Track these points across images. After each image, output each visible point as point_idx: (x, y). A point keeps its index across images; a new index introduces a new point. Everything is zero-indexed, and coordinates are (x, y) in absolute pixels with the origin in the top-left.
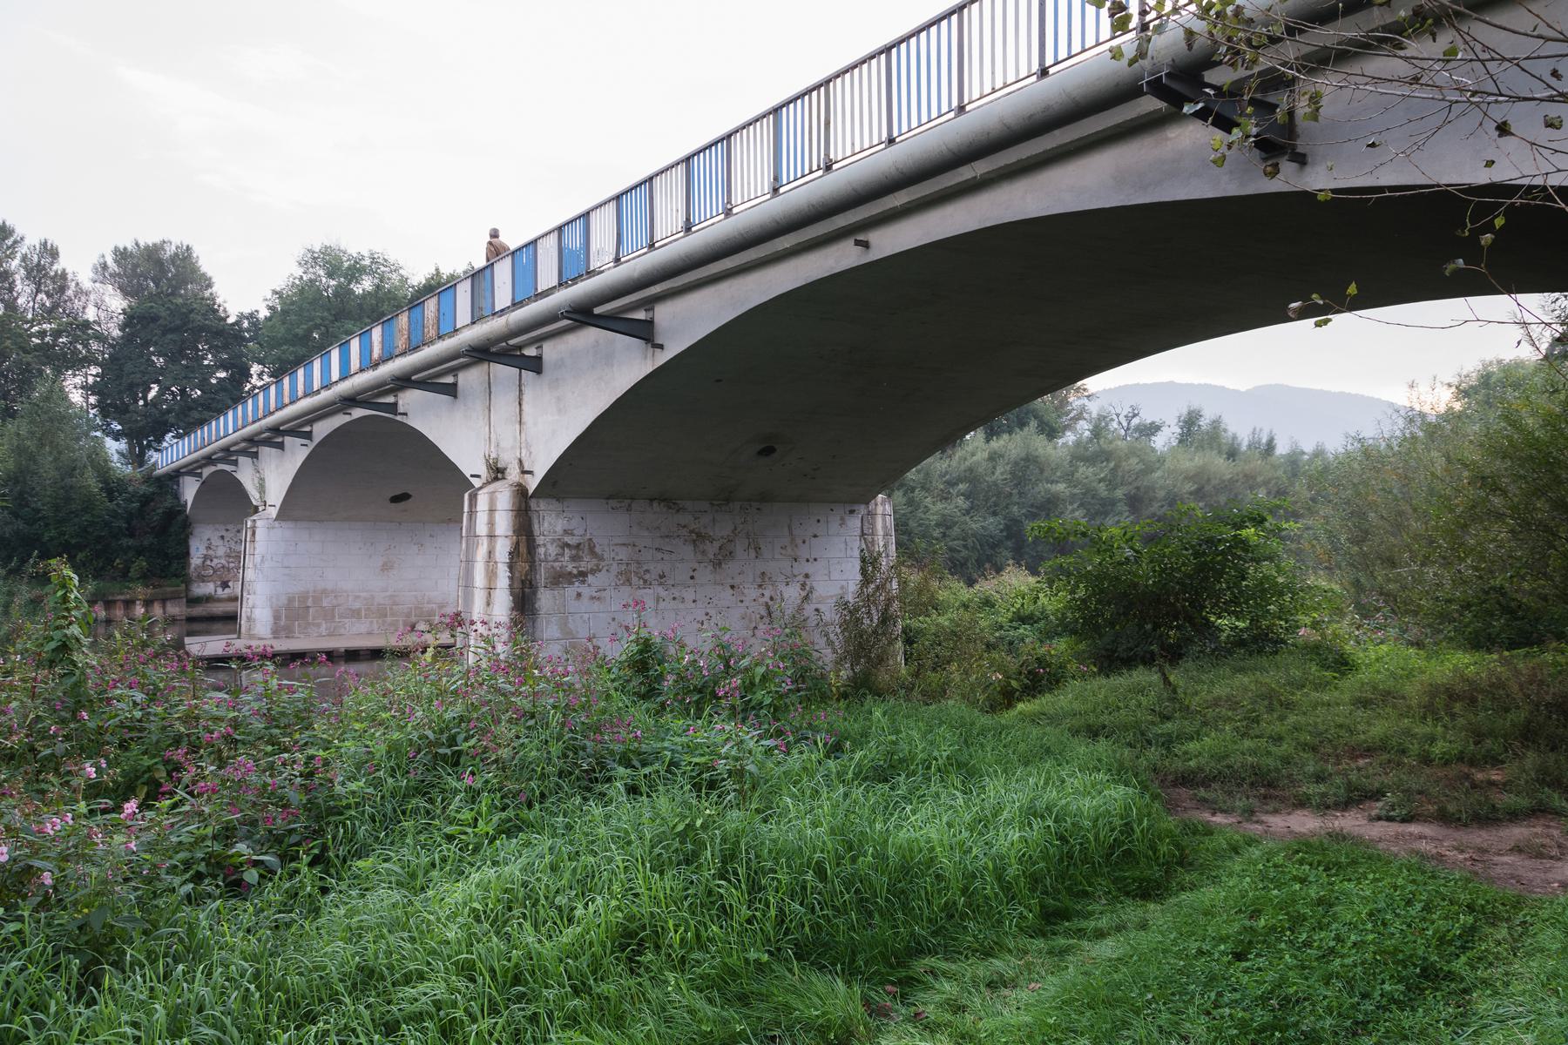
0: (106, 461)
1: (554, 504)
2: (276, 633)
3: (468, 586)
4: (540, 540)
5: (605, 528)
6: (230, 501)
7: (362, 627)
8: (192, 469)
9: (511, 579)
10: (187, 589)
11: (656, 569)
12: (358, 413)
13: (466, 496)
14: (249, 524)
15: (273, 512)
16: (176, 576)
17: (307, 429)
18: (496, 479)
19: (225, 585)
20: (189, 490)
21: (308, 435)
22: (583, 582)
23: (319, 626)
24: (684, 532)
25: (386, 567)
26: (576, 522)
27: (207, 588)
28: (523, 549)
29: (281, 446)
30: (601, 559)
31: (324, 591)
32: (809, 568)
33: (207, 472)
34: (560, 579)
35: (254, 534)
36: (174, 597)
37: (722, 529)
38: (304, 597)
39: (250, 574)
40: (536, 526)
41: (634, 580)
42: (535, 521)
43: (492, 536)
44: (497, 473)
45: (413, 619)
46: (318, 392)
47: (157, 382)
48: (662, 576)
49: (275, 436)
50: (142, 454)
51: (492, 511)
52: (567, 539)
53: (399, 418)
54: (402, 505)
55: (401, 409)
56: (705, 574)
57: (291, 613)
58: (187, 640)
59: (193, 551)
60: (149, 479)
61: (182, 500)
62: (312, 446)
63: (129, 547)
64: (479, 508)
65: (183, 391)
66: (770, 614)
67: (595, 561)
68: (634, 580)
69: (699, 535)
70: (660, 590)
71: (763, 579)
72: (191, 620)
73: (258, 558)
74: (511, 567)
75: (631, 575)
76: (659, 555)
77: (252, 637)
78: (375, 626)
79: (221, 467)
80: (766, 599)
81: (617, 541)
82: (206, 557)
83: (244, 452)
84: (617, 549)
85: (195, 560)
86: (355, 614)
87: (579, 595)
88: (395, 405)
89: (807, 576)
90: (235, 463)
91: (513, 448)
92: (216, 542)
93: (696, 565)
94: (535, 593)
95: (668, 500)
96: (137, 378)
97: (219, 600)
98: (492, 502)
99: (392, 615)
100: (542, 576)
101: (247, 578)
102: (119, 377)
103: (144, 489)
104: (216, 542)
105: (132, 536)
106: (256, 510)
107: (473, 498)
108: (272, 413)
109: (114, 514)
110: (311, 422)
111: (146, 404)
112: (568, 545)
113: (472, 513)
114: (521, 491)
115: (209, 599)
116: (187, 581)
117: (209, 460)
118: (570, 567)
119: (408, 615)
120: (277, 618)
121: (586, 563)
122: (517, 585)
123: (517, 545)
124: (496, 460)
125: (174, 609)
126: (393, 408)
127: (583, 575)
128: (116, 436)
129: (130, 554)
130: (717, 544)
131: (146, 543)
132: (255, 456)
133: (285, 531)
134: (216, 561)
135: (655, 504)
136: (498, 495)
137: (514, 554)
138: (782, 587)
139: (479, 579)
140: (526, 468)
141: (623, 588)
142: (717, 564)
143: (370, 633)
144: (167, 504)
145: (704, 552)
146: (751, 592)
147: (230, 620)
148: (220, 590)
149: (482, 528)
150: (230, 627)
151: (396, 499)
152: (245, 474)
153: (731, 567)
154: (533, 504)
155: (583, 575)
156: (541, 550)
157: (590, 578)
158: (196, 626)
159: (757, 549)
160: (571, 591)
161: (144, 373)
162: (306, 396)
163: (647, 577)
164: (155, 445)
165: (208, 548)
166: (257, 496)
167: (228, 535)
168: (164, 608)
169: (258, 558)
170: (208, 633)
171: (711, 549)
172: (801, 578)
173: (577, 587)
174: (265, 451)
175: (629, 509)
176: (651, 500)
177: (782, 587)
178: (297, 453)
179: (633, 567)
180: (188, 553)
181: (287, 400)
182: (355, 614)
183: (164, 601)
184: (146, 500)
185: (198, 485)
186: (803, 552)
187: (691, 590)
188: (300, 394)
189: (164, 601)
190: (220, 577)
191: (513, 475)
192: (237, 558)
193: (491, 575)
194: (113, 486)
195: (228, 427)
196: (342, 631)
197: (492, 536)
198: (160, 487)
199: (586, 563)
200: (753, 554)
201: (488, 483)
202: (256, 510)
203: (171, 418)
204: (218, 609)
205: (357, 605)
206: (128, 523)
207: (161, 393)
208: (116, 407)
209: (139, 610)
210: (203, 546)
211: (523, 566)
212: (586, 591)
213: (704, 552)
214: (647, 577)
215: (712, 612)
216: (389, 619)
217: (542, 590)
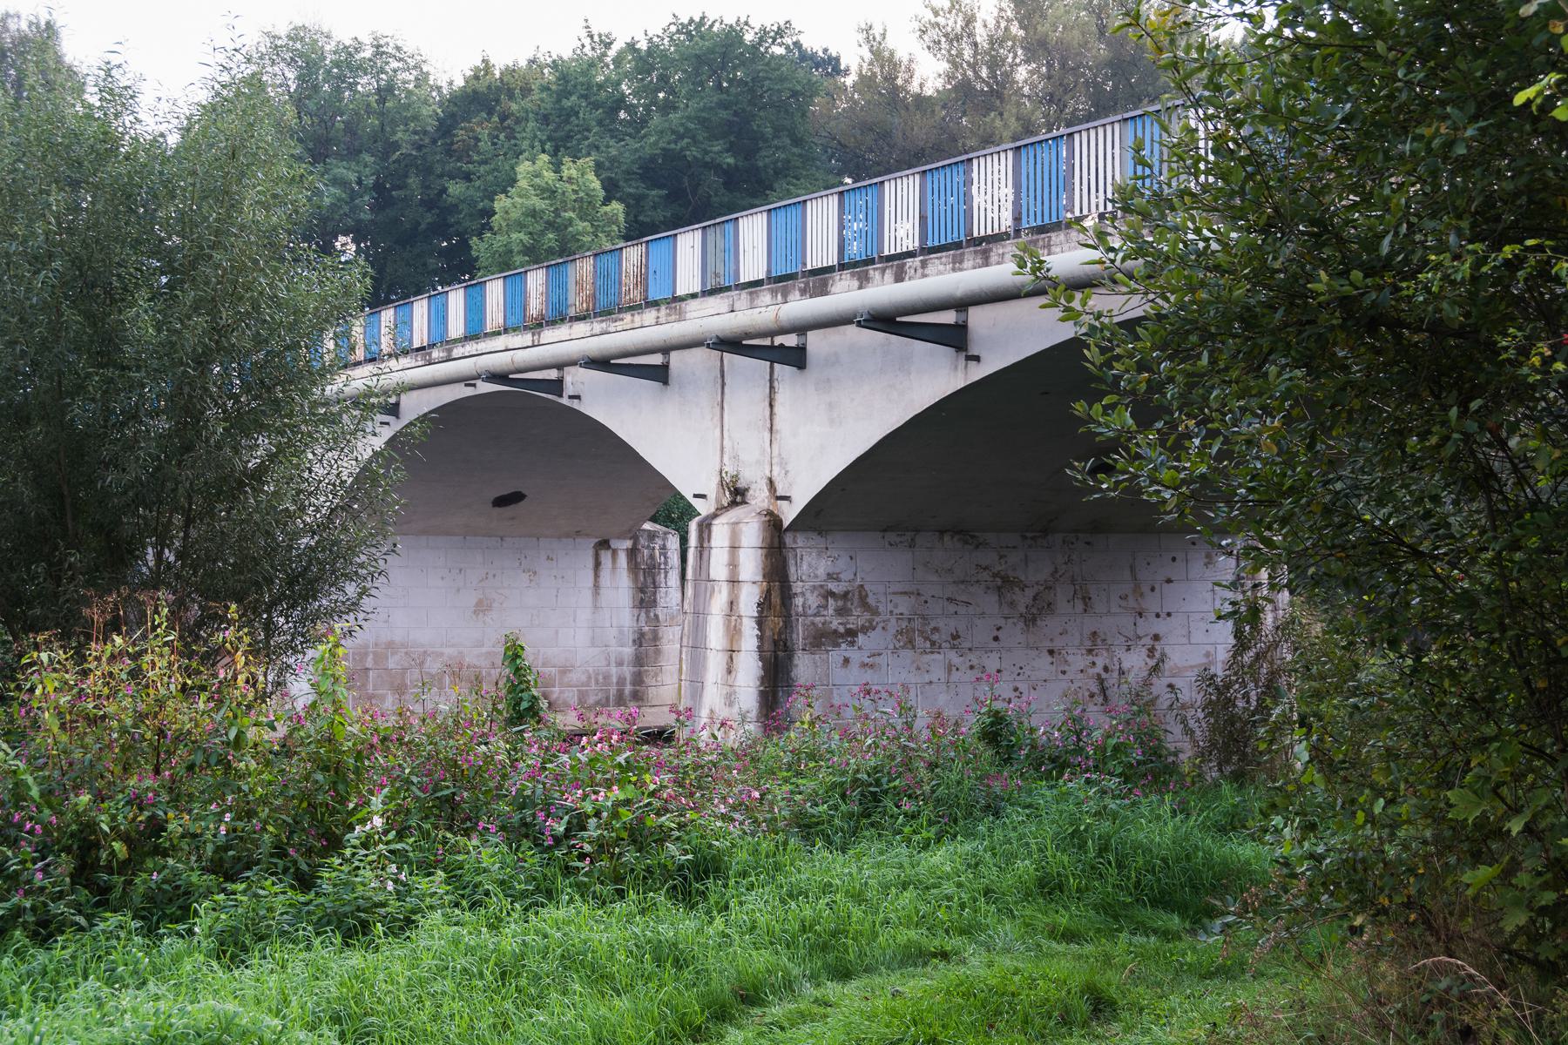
4: (797, 587)
5: (876, 569)
9: (761, 638)
11: (947, 626)
22: (852, 643)
24: (985, 575)
26: (843, 563)
28: (776, 599)
30: (875, 612)
32: (1160, 627)
34: (822, 639)
37: (1037, 572)
40: (792, 569)
41: (919, 641)
42: (791, 562)
43: (734, 582)
44: (737, 495)
48: (955, 637)
51: (734, 548)
52: (832, 586)
56: (1014, 633)
66: (1103, 690)
67: (867, 616)
68: (919, 641)
69: (1005, 579)
71: (1095, 642)
74: (760, 622)
76: (952, 608)
80: (1099, 669)
84: (898, 599)
87: (847, 661)
89: (1156, 637)
93: (1001, 622)
95: (964, 533)
100: (799, 635)
112: (832, 594)
114: (773, 523)
118: (835, 624)
121: (857, 619)
122: (768, 646)
124: (736, 478)
127: (851, 634)
130: (1030, 593)
135: (947, 538)
136: (743, 527)
137: (764, 605)
138: (1120, 653)
141: (903, 653)
142: (1030, 620)
145: (1012, 604)
146: (1078, 660)
153: (1050, 624)
154: (788, 539)
155: (851, 634)
156: (799, 601)
157: (861, 638)
159: (1086, 600)
160: (836, 656)
163: (935, 637)
171: (1023, 599)
172: (1148, 641)
173: (844, 650)
175: (912, 545)
176: (942, 532)
177: (1120, 653)
179: (917, 624)
186: (1151, 603)
187: (995, 656)
191: (759, 498)
193: (733, 632)
197: (734, 582)
199: (857, 619)
200: (1080, 606)
211: (775, 622)
212: (855, 656)
213: (1012, 604)
214: (935, 637)
215: (1023, 687)
217: (799, 653)
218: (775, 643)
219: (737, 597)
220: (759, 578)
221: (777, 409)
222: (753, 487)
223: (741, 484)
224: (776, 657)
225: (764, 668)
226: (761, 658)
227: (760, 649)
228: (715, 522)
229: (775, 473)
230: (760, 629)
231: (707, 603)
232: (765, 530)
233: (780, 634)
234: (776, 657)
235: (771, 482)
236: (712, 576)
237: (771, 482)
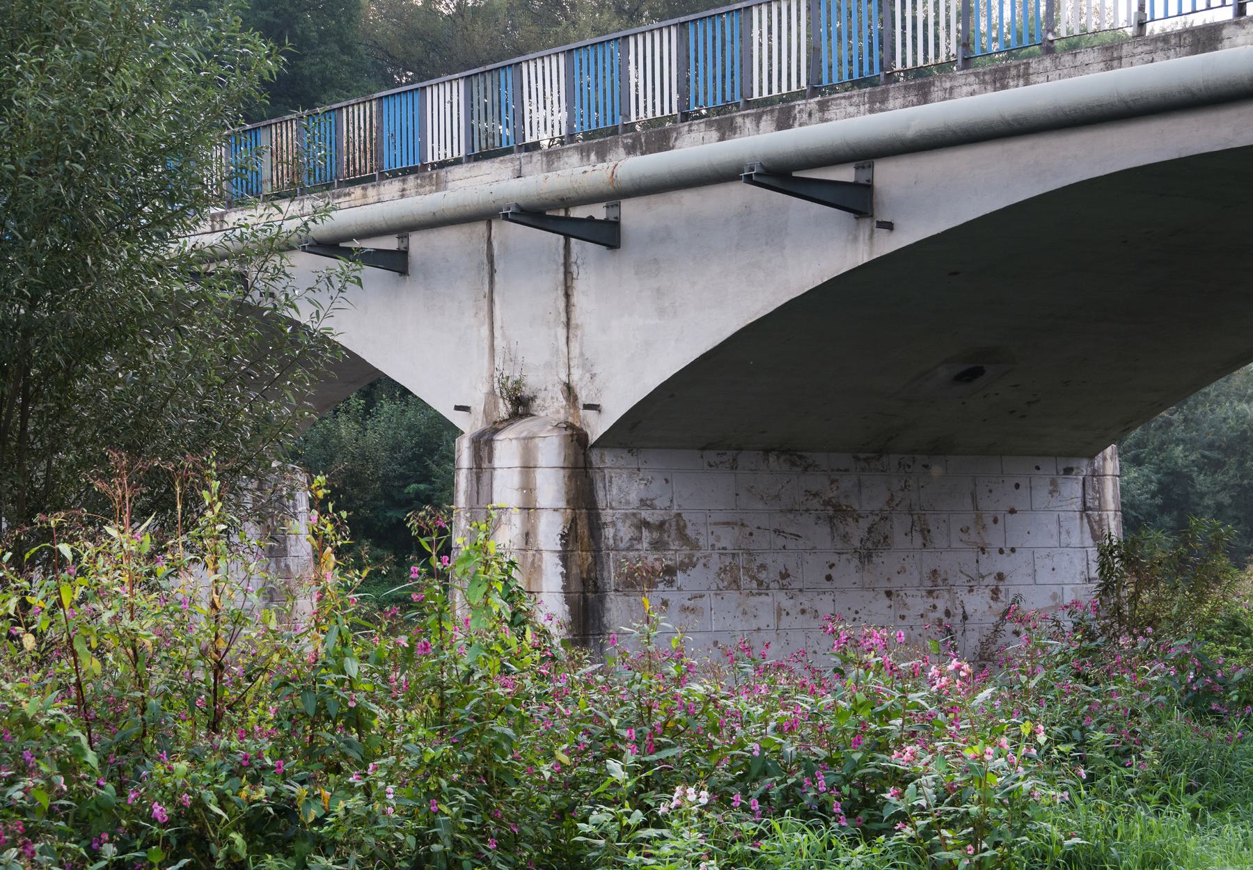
1: (625, 459)
4: (607, 516)
9: (566, 577)
22: (670, 583)
24: (815, 503)
28: (583, 529)
30: (695, 546)
37: (871, 501)
40: (600, 494)
41: (744, 580)
42: (599, 485)
48: (785, 575)
52: (646, 514)
56: (848, 571)
67: (686, 550)
68: (744, 580)
69: (838, 509)
70: (782, 598)
74: (565, 558)
75: (741, 575)
76: (780, 541)
81: (717, 517)
87: (665, 603)
93: (834, 558)
94: (601, 600)
95: (791, 452)
112: (646, 524)
122: (575, 586)
123: (573, 524)
127: (670, 571)
130: (864, 524)
136: (540, 443)
142: (865, 557)
145: (845, 537)
153: (887, 561)
154: (595, 456)
156: (609, 532)
159: (925, 532)
171: (857, 532)
175: (734, 466)
176: (767, 451)
179: (742, 560)
187: (827, 598)
211: (582, 557)
212: (674, 597)
213: (845, 537)
217: (612, 595)
220: (562, 504)
221: (574, 300)
224: (585, 599)
225: (571, 612)
226: (567, 601)
230: (565, 565)
232: (567, 446)
233: (589, 571)
234: (585, 599)
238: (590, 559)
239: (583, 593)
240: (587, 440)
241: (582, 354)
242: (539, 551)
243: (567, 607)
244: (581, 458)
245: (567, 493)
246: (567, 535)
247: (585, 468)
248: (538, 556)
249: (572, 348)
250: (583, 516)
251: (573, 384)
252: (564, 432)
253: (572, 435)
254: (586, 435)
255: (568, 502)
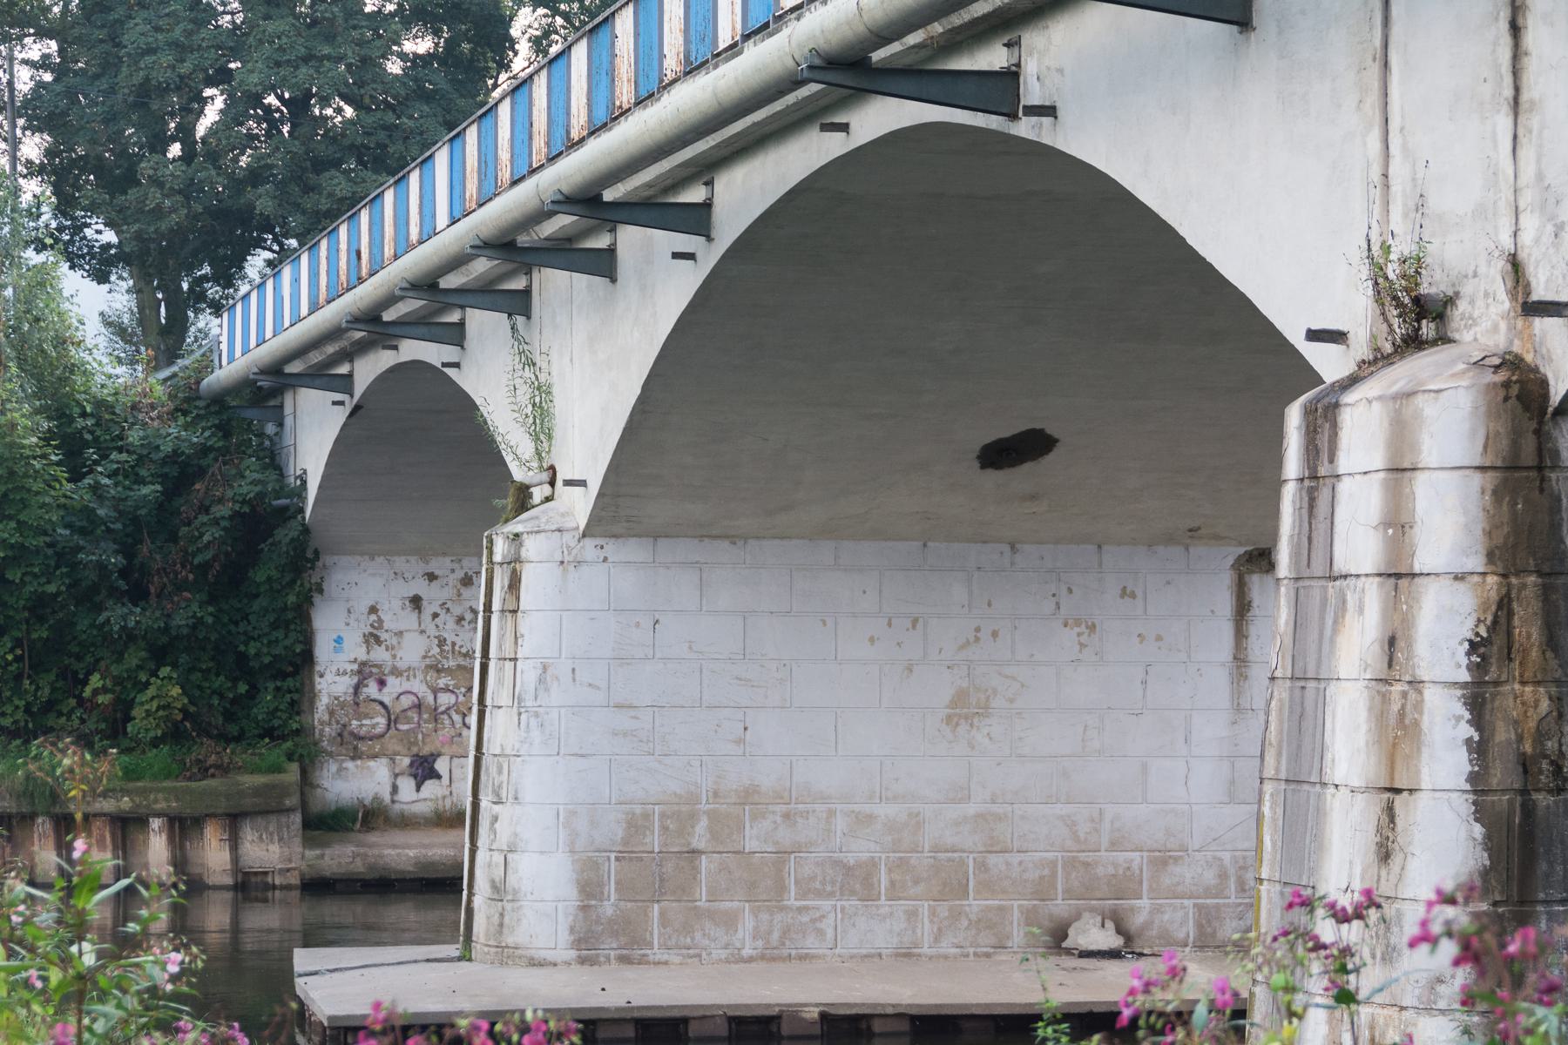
0: (61, 342)
2: (587, 948)
3: (1303, 779)
6: (438, 463)
7: (878, 929)
8: (319, 362)
9: (1479, 750)
10: (307, 781)
12: (879, 118)
13: (1294, 416)
14: (501, 549)
15: (578, 506)
16: (272, 734)
17: (695, 195)
18: (1413, 343)
19: (424, 769)
20: (313, 433)
21: (698, 220)
23: (730, 921)
25: (965, 710)
27: (356, 781)
29: (604, 265)
31: (749, 796)
33: (368, 370)
35: (514, 584)
36: (265, 808)
38: (681, 815)
39: (501, 730)
43: (1398, 576)
44: (1419, 316)
45: (1060, 907)
46: (734, 49)
47: (222, 77)
49: (584, 228)
50: (177, 326)
51: (1400, 471)
53: (1025, 128)
54: (1022, 477)
55: (1032, 93)
57: (638, 875)
58: (303, 959)
59: (323, 649)
60: (191, 402)
61: (292, 471)
62: (710, 255)
63: (129, 636)
64: (1347, 460)
65: (298, 106)
72: (317, 887)
73: (528, 673)
74: (1478, 701)
77: (506, 955)
78: (926, 928)
79: (413, 350)
82: (364, 672)
83: (486, 294)
85: (332, 682)
86: (856, 881)
88: (1011, 77)
90: (456, 335)
91: (1482, 212)
92: (396, 617)
96: (162, 66)
97: (406, 822)
98: (1401, 434)
99: (987, 887)
101: (491, 747)
102: (109, 66)
103: (175, 435)
104: (396, 617)
105: (138, 595)
106: (523, 499)
107: (1323, 421)
108: (574, 145)
109: (85, 523)
110: (705, 170)
111: (188, 157)
113: (1318, 481)
115: (372, 817)
116: (308, 758)
117: (373, 326)
119: (1043, 890)
120: (589, 889)
122: (1502, 774)
123: (1502, 613)
124: (1415, 266)
125: (267, 850)
126: (1002, 90)
128: (100, 267)
129: (133, 658)
131: (180, 620)
132: (520, 305)
133: (620, 571)
134: (394, 685)
136: (1427, 407)
139: (1348, 749)
140: (1540, 293)
143: (906, 955)
144: (245, 488)
147: (435, 894)
148: (407, 786)
149: (1357, 543)
150: (434, 915)
151: (1006, 453)
152: (488, 372)
158: (333, 910)
161: (181, 49)
162: (691, 69)
164: (213, 291)
165: (372, 639)
166: (526, 448)
167: (433, 595)
168: (234, 843)
169: (528, 673)
170: (370, 935)
174: (555, 286)
178: (660, 283)
180: (306, 659)
181: (625, 95)
182: (856, 881)
183: (234, 821)
184: (181, 473)
185: (339, 416)
188: (672, 64)
189: (234, 821)
190: (408, 740)
191: (1485, 323)
192: (464, 672)
193: (1397, 733)
194: (81, 429)
195: (431, 212)
196: (811, 943)
197: (1398, 576)
198: (225, 430)
201: (1378, 360)
202: (523, 499)
203: (264, 202)
204: (401, 852)
205: (860, 850)
206: (128, 551)
207: (232, 116)
208: (100, 168)
209: (157, 848)
210: (360, 631)
216: (974, 904)
218: (1526, 765)
219: (1407, 622)
220: (1475, 562)
221: (1530, 39)
222: (1467, 289)
223: (1431, 286)
224: (1528, 810)
225: (1490, 843)
226: (1481, 813)
227: (1478, 783)
228: (1349, 397)
229: (1526, 238)
230: (1478, 721)
231: (1327, 644)
232: (1492, 414)
233: (1540, 736)
234: (1528, 810)
235: (1515, 265)
236: (1340, 565)
237: (1515, 265)
238: (1545, 705)
239: (1524, 792)
240: (1545, 396)
241: (1540, 176)
242: (1415, 683)
243: (1478, 830)
244: (1529, 444)
245: (1489, 534)
246: (1485, 642)
247: (1540, 468)
248: (1412, 695)
249: (1522, 163)
250: (1529, 593)
251: (1522, 255)
252: (1491, 377)
253: (1506, 385)
254: (1544, 383)
255: (1491, 556)
